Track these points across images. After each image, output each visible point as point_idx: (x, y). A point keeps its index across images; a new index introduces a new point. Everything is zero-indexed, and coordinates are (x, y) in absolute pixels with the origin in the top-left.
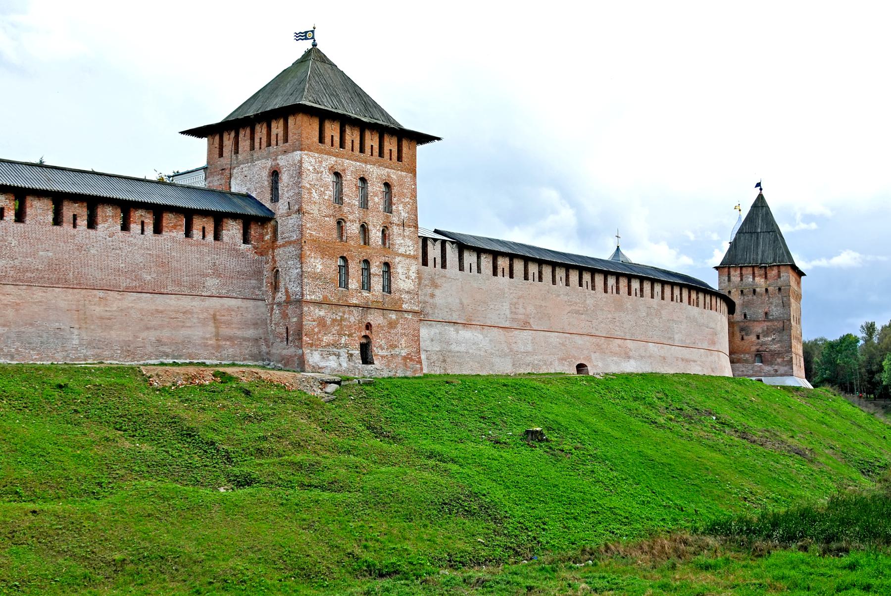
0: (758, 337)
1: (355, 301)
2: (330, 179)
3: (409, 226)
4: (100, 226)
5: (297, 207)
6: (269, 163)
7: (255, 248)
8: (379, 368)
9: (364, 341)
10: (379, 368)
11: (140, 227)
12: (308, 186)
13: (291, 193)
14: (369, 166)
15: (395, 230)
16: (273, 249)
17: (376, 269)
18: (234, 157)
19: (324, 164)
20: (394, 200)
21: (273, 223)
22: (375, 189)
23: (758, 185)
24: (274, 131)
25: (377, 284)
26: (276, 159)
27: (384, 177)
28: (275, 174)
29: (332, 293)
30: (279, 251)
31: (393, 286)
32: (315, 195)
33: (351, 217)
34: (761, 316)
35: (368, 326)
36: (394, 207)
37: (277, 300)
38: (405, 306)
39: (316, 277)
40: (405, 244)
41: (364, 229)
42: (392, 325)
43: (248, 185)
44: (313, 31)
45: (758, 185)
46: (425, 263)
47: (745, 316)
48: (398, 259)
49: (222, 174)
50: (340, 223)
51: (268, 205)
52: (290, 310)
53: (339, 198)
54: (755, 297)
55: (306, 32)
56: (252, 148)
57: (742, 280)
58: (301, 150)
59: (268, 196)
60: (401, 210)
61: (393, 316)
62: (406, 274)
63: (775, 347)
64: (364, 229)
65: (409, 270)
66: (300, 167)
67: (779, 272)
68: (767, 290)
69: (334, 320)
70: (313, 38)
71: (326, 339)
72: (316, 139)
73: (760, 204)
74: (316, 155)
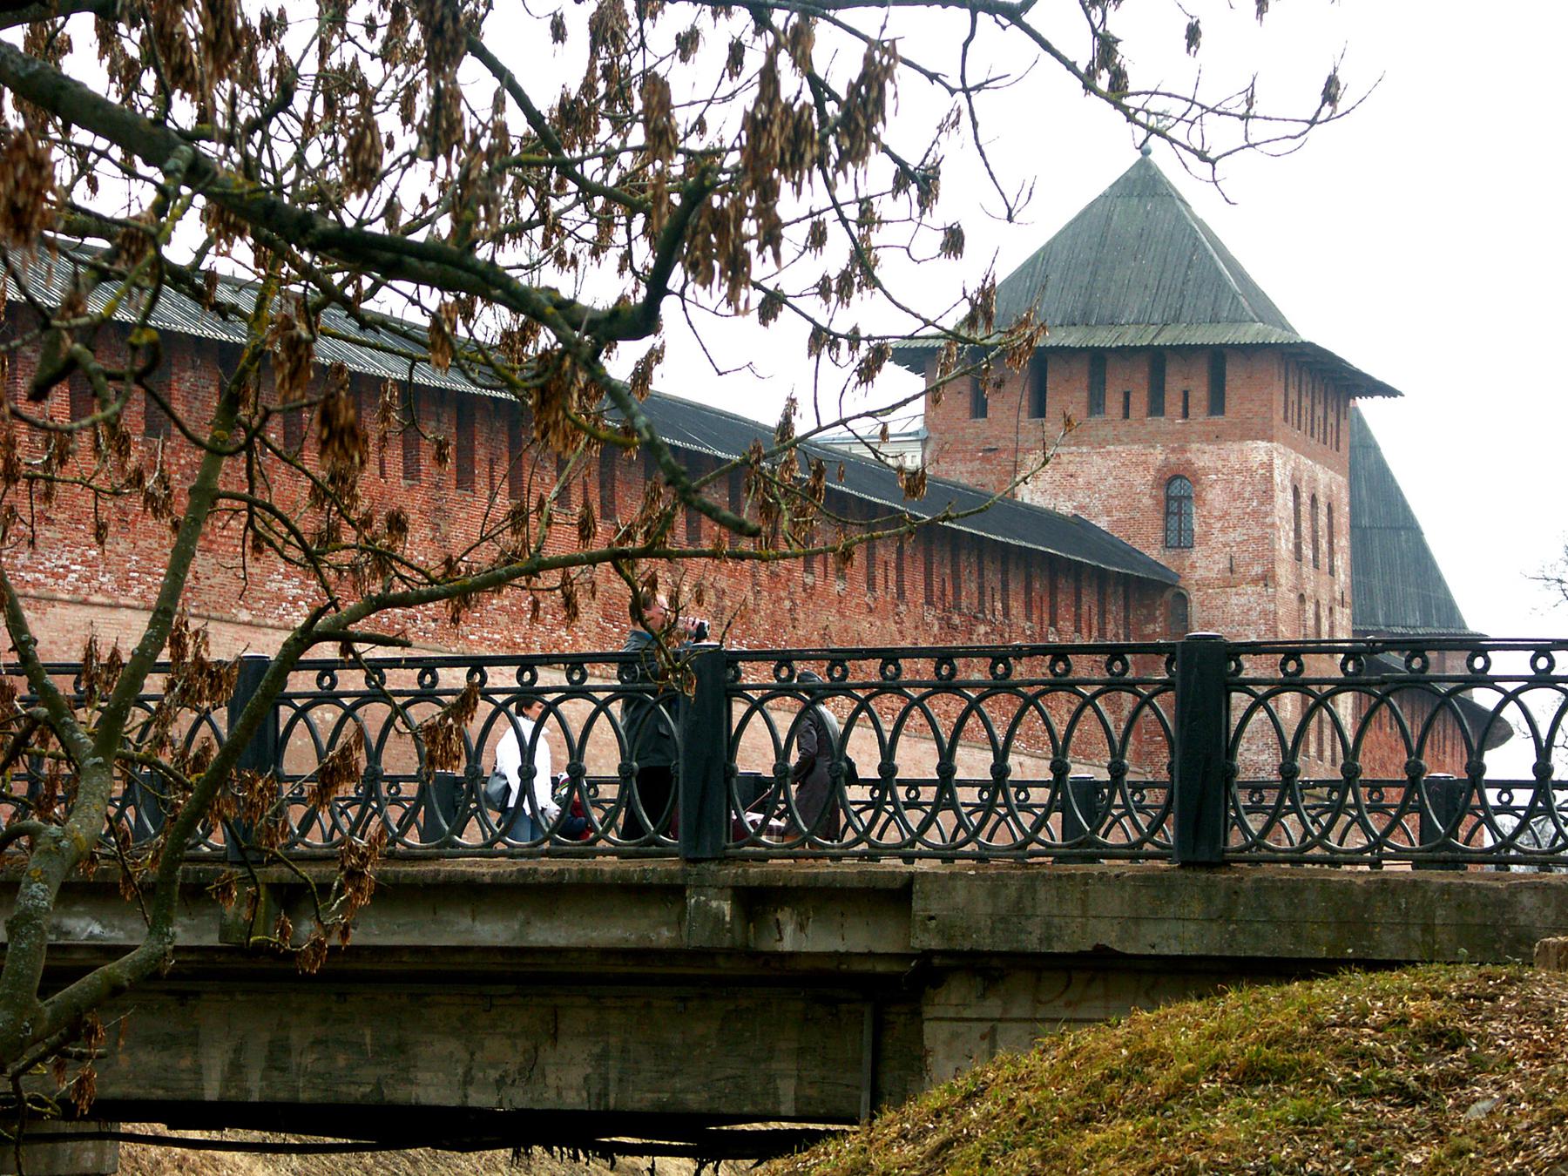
5: (1257, 569)
6: (1158, 456)
18: (1027, 422)
21: (1168, 595)
24: (1174, 386)
26: (1184, 451)
33: (1309, 590)
43: (1081, 497)
49: (983, 459)
51: (1154, 553)
53: (1298, 547)
56: (1096, 405)
58: (1271, 440)
66: (1269, 479)
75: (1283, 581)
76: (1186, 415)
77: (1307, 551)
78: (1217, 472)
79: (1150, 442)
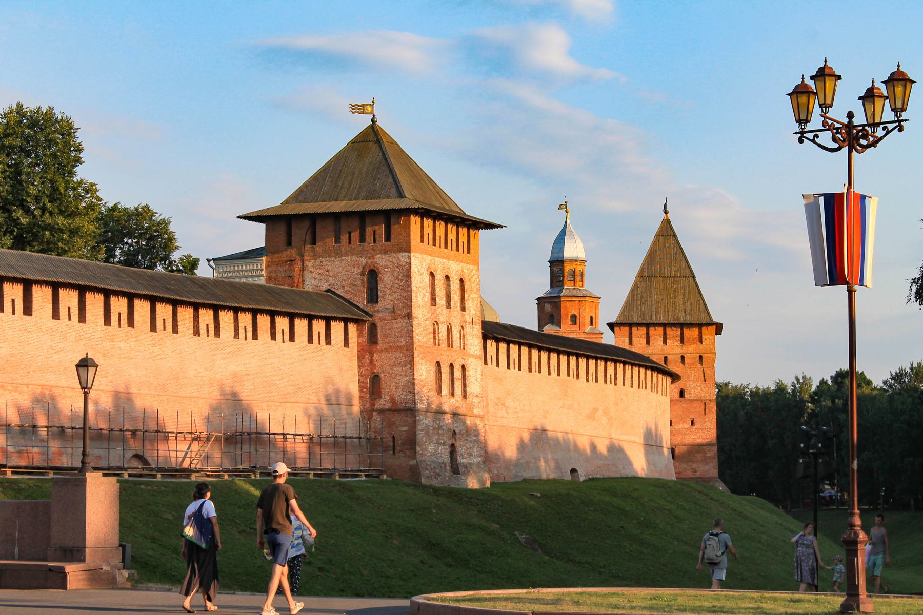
2: (427, 278)
5: (405, 311)
6: (363, 261)
13: (396, 296)
15: (468, 328)
16: (371, 354)
17: (458, 374)
19: (424, 264)
22: (455, 286)
26: (374, 258)
28: (373, 275)
31: (468, 389)
32: (420, 298)
33: (442, 319)
41: (449, 331)
44: (372, 106)
46: (486, 363)
52: (397, 418)
53: (433, 300)
55: (364, 105)
56: (338, 240)
57: (648, 343)
64: (449, 331)
67: (700, 333)
68: (683, 357)
72: (419, 239)
73: (666, 232)
74: (420, 256)
75: (420, 316)
76: (375, 242)
77: (441, 300)
78: (387, 267)
79: (360, 254)
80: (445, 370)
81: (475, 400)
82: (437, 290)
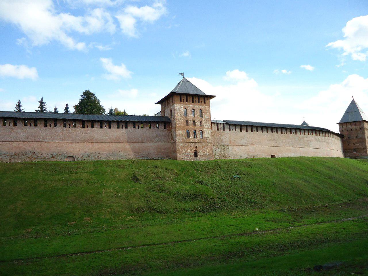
0: (354, 144)
1: (192, 141)
2: (183, 110)
3: (208, 120)
4: (128, 128)
7: (167, 129)
8: (200, 158)
9: (195, 151)
10: (200, 158)
11: (138, 127)
12: (177, 113)
14: (195, 106)
15: (204, 122)
20: (203, 114)
22: (197, 111)
23: (352, 97)
24: (171, 100)
25: (199, 136)
27: (200, 108)
28: (171, 111)
29: (185, 139)
30: (172, 130)
31: (204, 136)
32: (179, 115)
34: (354, 137)
35: (196, 147)
36: (203, 116)
37: (172, 142)
38: (207, 142)
39: (180, 135)
40: (207, 125)
41: (194, 122)
42: (203, 147)
45: (352, 97)
47: (349, 138)
48: (205, 129)
50: (187, 121)
54: (352, 132)
57: (347, 127)
59: (170, 116)
60: (205, 116)
61: (204, 144)
62: (208, 134)
63: (360, 147)
64: (194, 122)
65: (208, 132)
68: (356, 129)
69: (185, 146)
70: (183, 75)
71: (183, 151)
80: (191, 133)
81: (208, 139)
82: (188, 113)
